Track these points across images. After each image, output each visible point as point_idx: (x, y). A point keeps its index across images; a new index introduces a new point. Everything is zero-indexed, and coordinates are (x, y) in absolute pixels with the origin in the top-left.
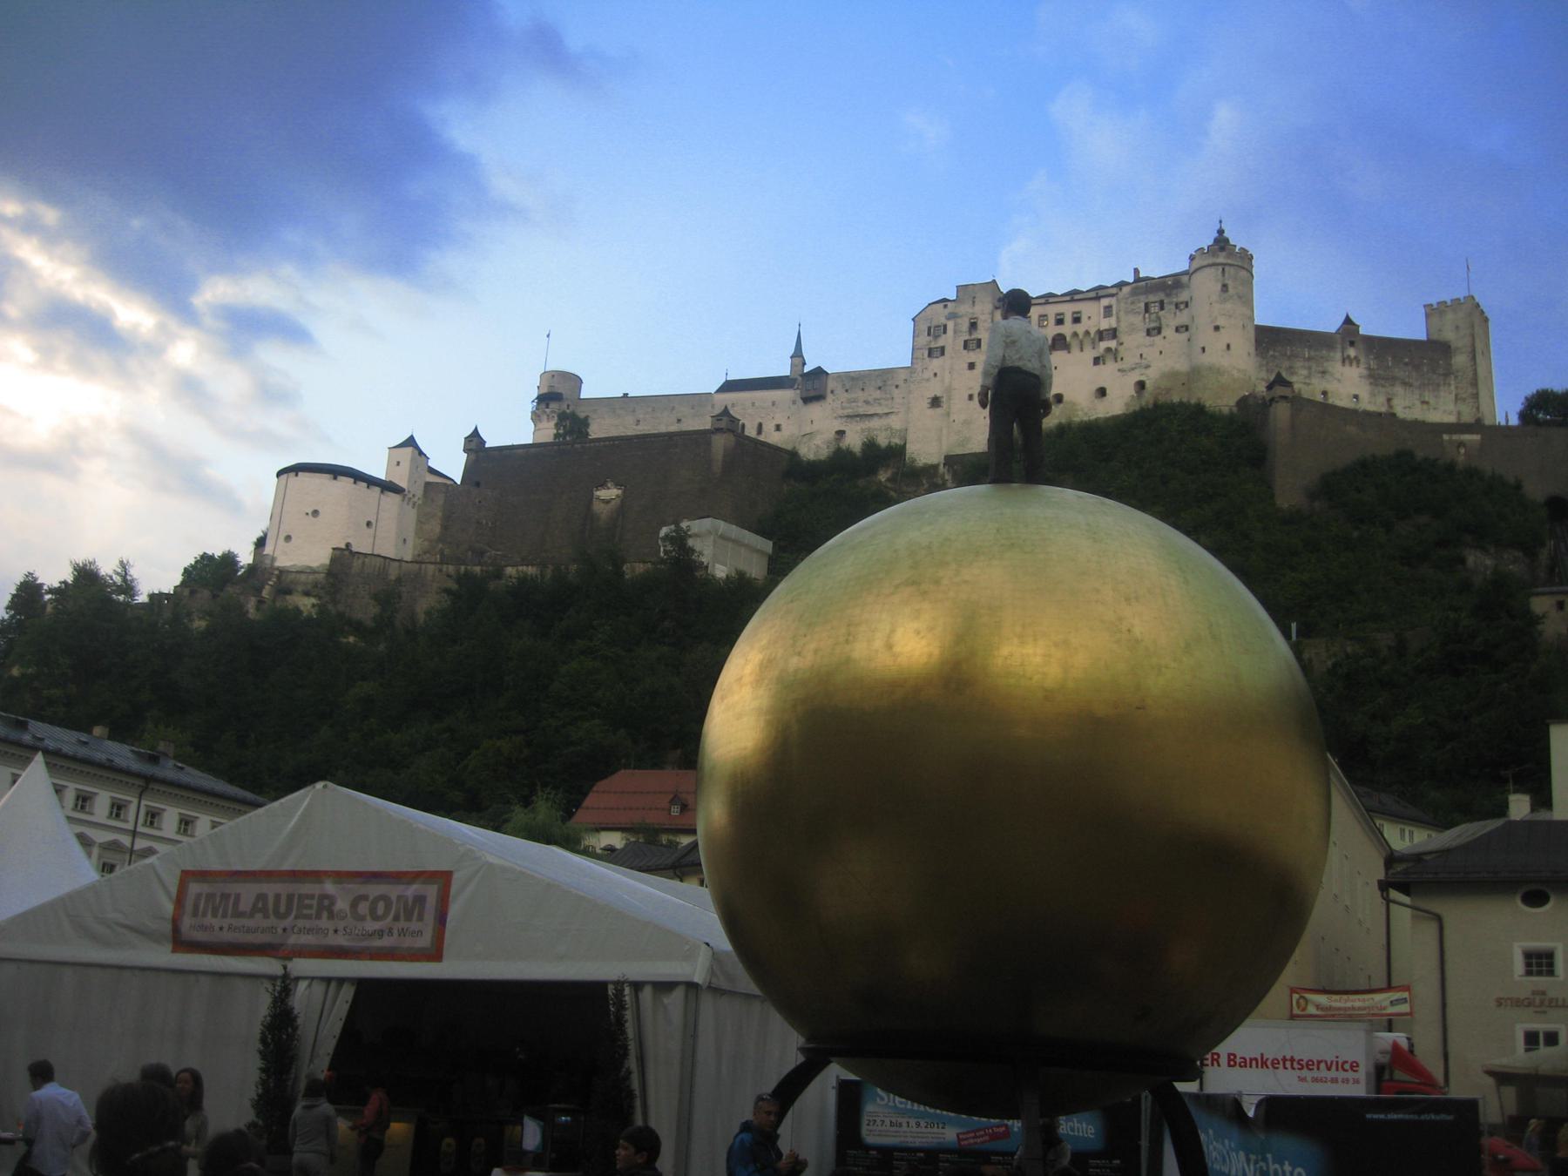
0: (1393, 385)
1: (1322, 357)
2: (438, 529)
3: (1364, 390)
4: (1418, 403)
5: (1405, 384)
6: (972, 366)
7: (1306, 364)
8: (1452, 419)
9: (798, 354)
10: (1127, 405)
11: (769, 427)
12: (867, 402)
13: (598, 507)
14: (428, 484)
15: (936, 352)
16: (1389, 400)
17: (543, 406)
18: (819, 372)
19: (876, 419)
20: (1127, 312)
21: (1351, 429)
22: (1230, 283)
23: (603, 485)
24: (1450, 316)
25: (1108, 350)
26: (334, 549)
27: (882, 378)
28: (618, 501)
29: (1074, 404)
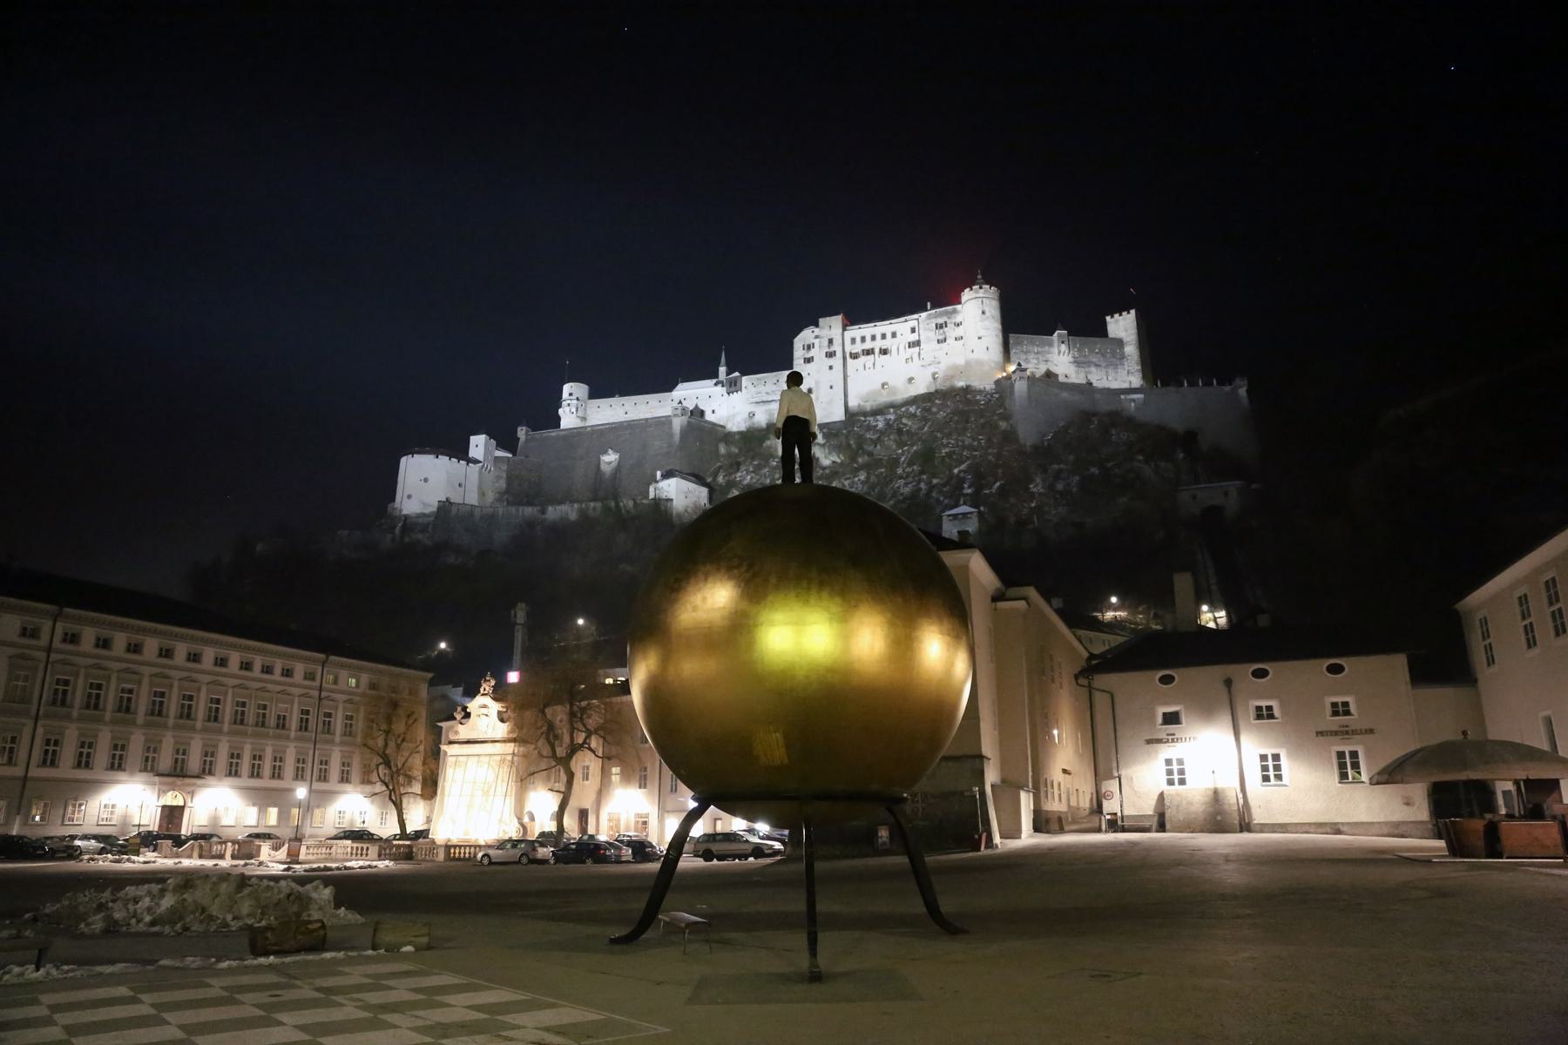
0: (1089, 367)
1: (1045, 352)
2: (504, 485)
5: (1097, 366)
6: (831, 368)
7: (1036, 356)
8: (1126, 386)
10: (928, 388)
12: (767, 393)
13: (603, 467)
15: (808, 360)
20: (925, 330)
21: (1065, 395)
23: (605, 452)
24: (1121, 323)
26: (439, 501)
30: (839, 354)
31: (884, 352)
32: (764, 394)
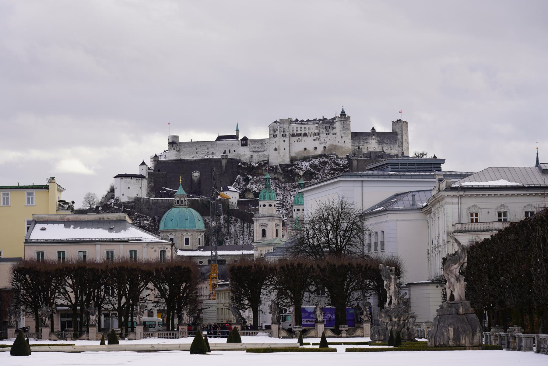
2: (153, 185)
3: (376, 146)
4: (389, 148)
5: (386, 143)
6: (284, 141)
9: (237, 131)
11: (232, 151)
12: (258, 148)
13: (193, 178)
16: (382, 148)
17: (171, 145)
18: (245, 139)
19: (261, 152)
22: (345, 125)
24: (397, 125)
25: (317, 138)
28: (199, 176)
29: (309, 150)
30: (288, 136)
31: (305, 135)
32: (257, 148)
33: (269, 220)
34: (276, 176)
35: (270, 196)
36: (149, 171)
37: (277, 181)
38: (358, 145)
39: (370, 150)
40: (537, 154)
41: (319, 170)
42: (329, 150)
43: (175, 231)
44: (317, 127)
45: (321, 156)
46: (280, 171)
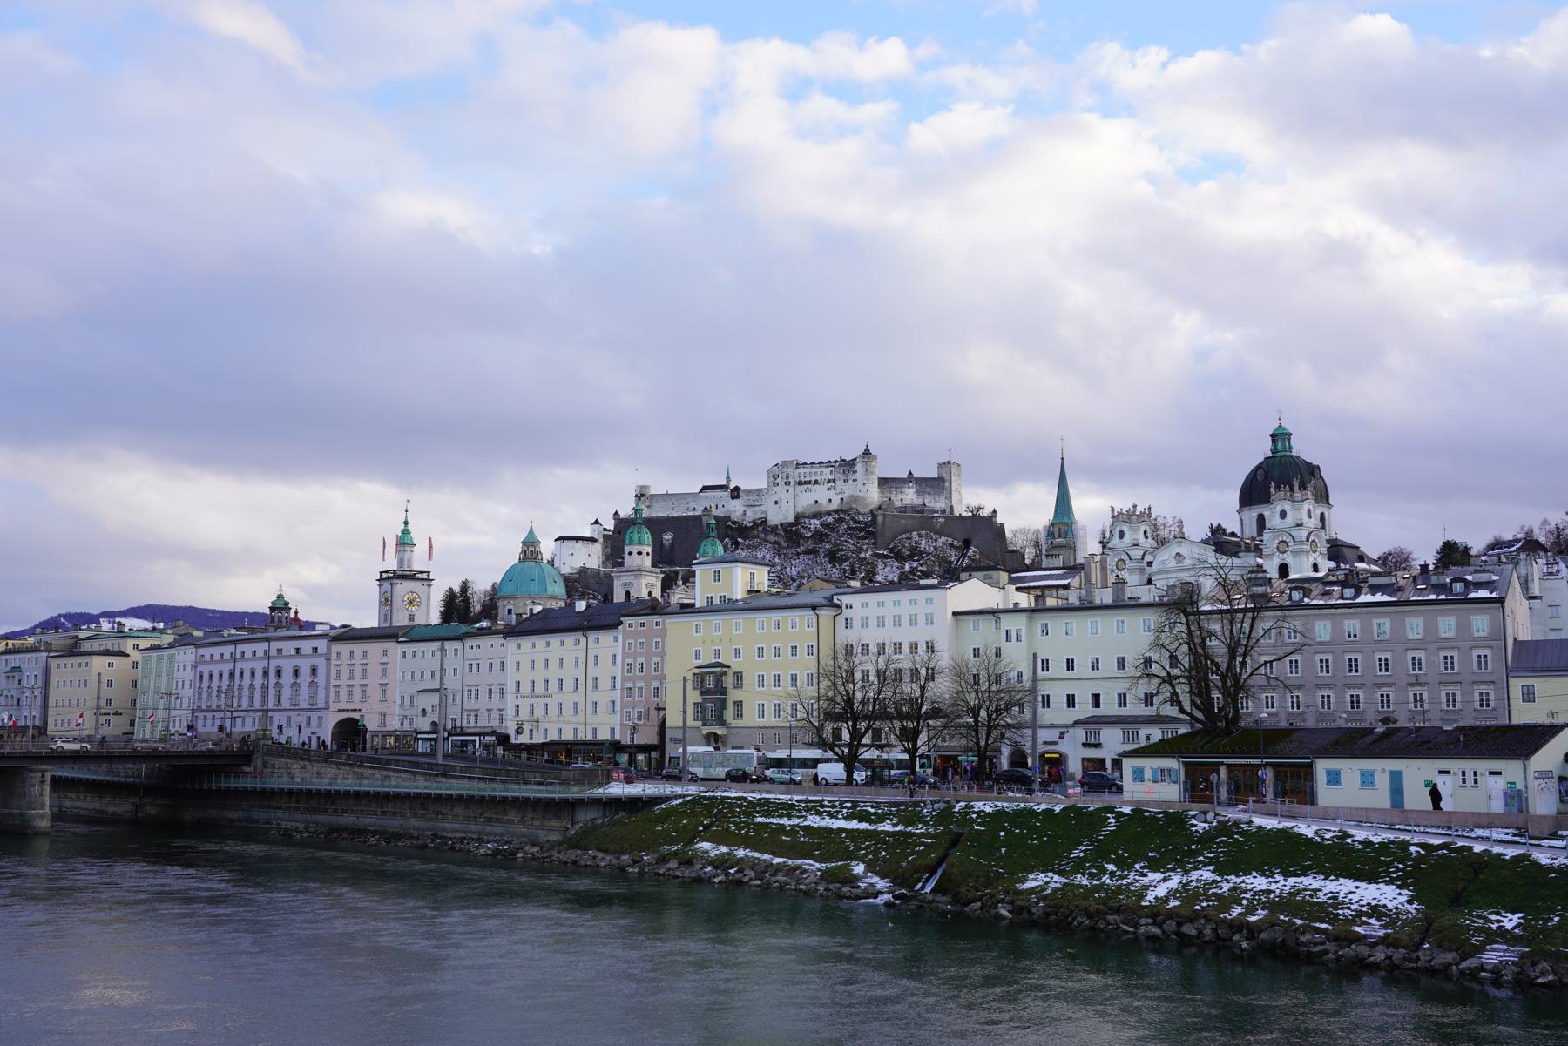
3: (914, 497)
5: (929, 494)
6: (787, 491)
9: (728, 478)
13: (664, 542)
14: (604, 535)
18: (737, 489)
27: (759, 492)
30: (792, 484)
31: (816, 482)
33: (635, 576)
34: (776, 539)
35: (639, 538)
36: (606, 533)
37: (777, 546)
38: (888, 495)
39: (905, 502)
40: (1062, 459)
41: (832, 530)
42: (847, 503)
43: (514, 597)
44: (831, 471)
45: (836, 511)
46: (781, 532)
